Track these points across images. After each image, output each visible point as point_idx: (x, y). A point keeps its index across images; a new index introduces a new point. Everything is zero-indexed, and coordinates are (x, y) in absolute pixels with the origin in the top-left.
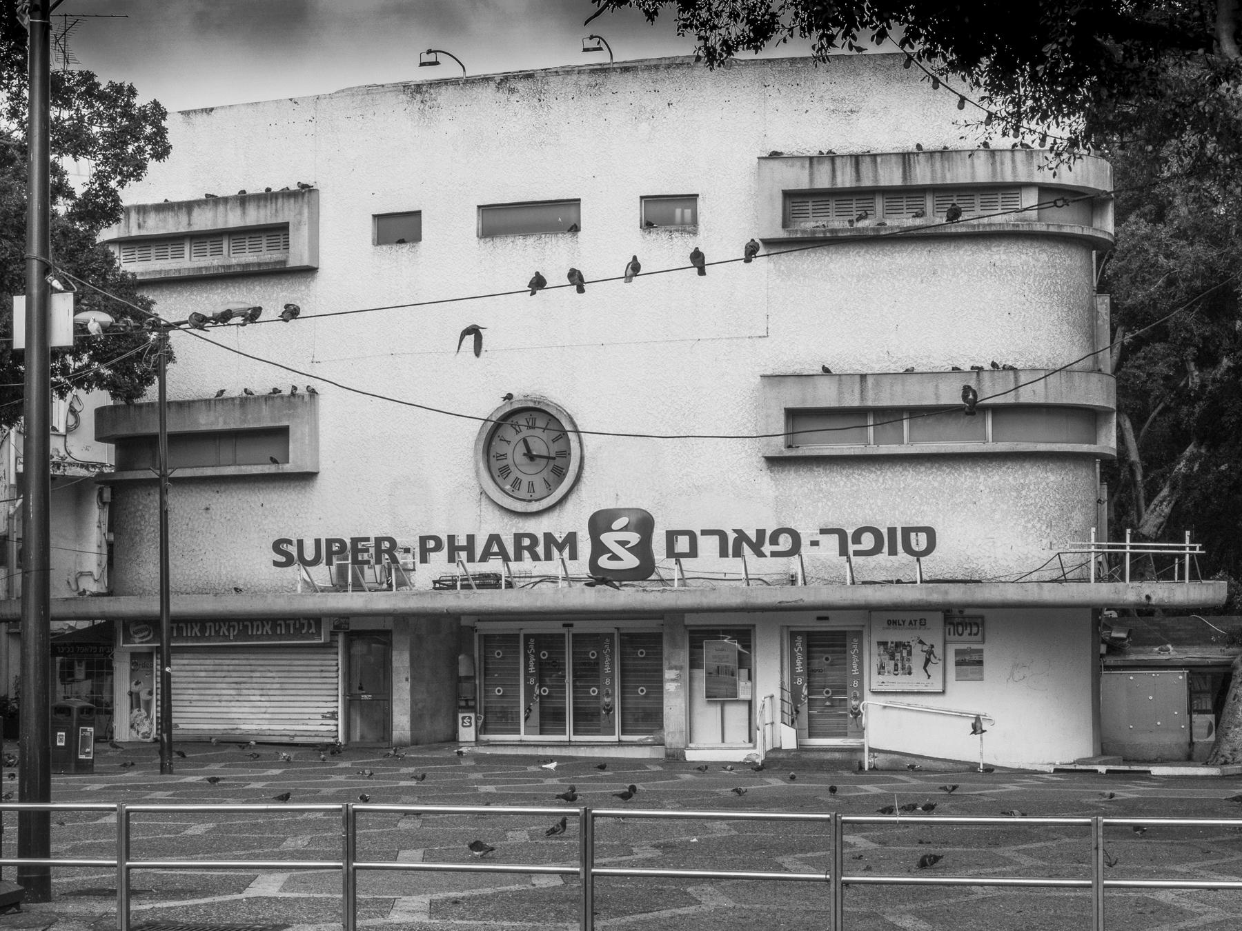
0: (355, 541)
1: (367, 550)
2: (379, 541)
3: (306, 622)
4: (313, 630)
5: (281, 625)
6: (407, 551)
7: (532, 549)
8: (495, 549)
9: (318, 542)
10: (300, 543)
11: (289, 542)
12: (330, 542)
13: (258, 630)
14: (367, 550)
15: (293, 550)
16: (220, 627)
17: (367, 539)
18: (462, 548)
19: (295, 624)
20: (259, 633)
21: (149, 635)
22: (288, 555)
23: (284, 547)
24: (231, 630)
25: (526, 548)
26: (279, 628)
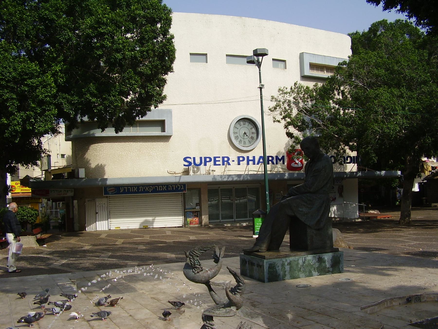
0: (215, 158)
1: (219, 161)
2: (223, 158)
3: (180, 186)
4: (183, 188)
5: (170, 187)
6: (233, 161)
7: (272, 161)
8: (261, 161)
9: (201, 158)
10: (194, 158)
11: (190, 158)
12: (205, 158)
13: (161, 189)
14: (219, 161)
15: (191, 160)
16: (134, 189)
17: (219, 157)
18: (251, 160)
19: (175, 187)
20: (161, 190)
21: (115, 191)
22: (190, 164)
23: (188, 159)
24: (150, 189)
25: (270, 160)
26: (169, 188)
